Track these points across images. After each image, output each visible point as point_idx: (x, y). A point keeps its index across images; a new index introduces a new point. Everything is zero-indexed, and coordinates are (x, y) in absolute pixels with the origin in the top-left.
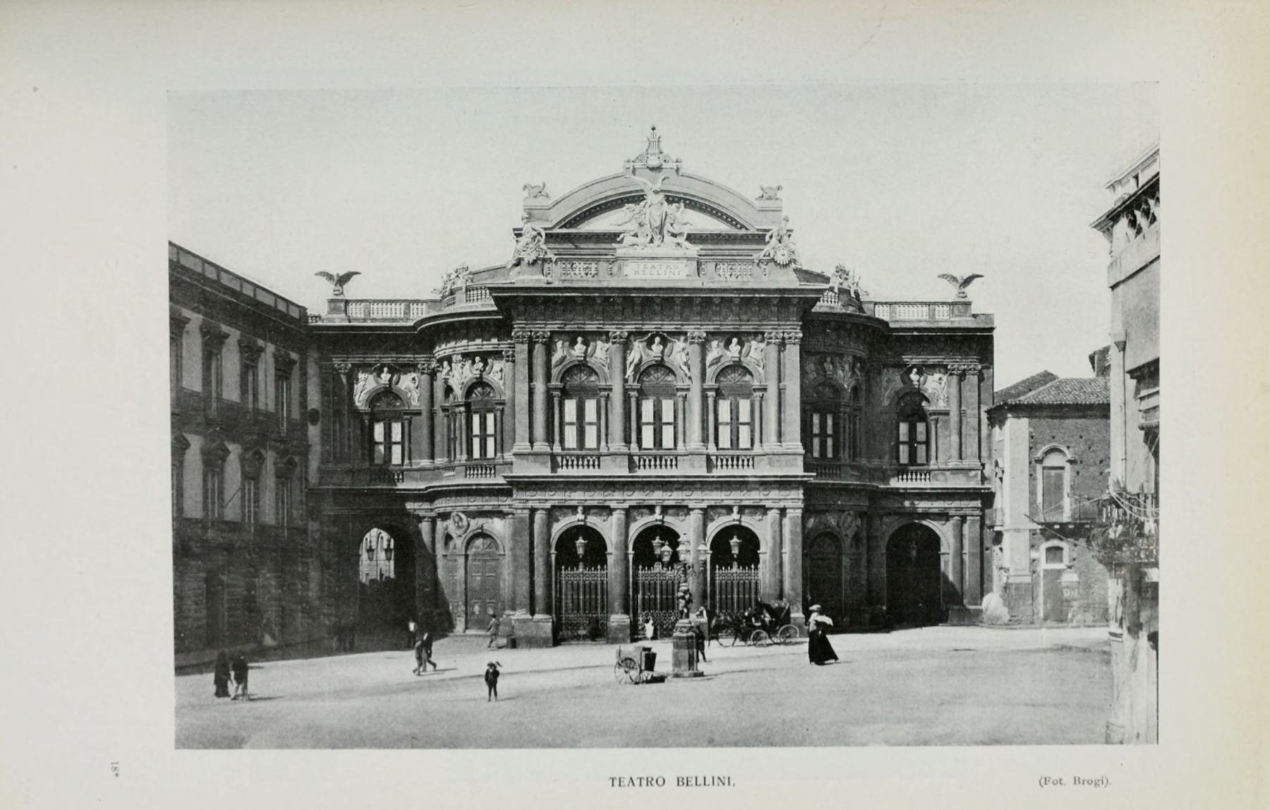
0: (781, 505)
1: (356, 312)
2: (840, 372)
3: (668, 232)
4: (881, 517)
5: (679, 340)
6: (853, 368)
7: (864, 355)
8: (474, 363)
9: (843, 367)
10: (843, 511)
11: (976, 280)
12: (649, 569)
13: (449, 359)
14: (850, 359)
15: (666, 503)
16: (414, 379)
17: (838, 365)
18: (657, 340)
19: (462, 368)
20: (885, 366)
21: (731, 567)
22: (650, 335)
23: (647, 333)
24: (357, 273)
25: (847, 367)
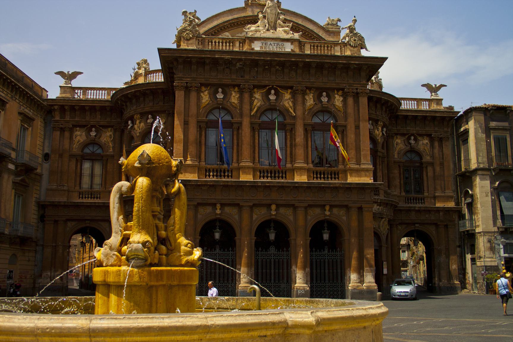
1: (79, 95)
2: (376, 131)
3: (280, 25)
5: (287, 93)
6: (382, 130)
7: (387, 123)
8: (148, 118)
9: (378, 128)
11: (443, 88)
12: (266, 251)
14: (382, 124)
16: (111, 135)
17: (375, 127)
18: (273, 92)
19: (140, 123)
23: (265, 87)
24: (81, 73)
25: (380, 128)
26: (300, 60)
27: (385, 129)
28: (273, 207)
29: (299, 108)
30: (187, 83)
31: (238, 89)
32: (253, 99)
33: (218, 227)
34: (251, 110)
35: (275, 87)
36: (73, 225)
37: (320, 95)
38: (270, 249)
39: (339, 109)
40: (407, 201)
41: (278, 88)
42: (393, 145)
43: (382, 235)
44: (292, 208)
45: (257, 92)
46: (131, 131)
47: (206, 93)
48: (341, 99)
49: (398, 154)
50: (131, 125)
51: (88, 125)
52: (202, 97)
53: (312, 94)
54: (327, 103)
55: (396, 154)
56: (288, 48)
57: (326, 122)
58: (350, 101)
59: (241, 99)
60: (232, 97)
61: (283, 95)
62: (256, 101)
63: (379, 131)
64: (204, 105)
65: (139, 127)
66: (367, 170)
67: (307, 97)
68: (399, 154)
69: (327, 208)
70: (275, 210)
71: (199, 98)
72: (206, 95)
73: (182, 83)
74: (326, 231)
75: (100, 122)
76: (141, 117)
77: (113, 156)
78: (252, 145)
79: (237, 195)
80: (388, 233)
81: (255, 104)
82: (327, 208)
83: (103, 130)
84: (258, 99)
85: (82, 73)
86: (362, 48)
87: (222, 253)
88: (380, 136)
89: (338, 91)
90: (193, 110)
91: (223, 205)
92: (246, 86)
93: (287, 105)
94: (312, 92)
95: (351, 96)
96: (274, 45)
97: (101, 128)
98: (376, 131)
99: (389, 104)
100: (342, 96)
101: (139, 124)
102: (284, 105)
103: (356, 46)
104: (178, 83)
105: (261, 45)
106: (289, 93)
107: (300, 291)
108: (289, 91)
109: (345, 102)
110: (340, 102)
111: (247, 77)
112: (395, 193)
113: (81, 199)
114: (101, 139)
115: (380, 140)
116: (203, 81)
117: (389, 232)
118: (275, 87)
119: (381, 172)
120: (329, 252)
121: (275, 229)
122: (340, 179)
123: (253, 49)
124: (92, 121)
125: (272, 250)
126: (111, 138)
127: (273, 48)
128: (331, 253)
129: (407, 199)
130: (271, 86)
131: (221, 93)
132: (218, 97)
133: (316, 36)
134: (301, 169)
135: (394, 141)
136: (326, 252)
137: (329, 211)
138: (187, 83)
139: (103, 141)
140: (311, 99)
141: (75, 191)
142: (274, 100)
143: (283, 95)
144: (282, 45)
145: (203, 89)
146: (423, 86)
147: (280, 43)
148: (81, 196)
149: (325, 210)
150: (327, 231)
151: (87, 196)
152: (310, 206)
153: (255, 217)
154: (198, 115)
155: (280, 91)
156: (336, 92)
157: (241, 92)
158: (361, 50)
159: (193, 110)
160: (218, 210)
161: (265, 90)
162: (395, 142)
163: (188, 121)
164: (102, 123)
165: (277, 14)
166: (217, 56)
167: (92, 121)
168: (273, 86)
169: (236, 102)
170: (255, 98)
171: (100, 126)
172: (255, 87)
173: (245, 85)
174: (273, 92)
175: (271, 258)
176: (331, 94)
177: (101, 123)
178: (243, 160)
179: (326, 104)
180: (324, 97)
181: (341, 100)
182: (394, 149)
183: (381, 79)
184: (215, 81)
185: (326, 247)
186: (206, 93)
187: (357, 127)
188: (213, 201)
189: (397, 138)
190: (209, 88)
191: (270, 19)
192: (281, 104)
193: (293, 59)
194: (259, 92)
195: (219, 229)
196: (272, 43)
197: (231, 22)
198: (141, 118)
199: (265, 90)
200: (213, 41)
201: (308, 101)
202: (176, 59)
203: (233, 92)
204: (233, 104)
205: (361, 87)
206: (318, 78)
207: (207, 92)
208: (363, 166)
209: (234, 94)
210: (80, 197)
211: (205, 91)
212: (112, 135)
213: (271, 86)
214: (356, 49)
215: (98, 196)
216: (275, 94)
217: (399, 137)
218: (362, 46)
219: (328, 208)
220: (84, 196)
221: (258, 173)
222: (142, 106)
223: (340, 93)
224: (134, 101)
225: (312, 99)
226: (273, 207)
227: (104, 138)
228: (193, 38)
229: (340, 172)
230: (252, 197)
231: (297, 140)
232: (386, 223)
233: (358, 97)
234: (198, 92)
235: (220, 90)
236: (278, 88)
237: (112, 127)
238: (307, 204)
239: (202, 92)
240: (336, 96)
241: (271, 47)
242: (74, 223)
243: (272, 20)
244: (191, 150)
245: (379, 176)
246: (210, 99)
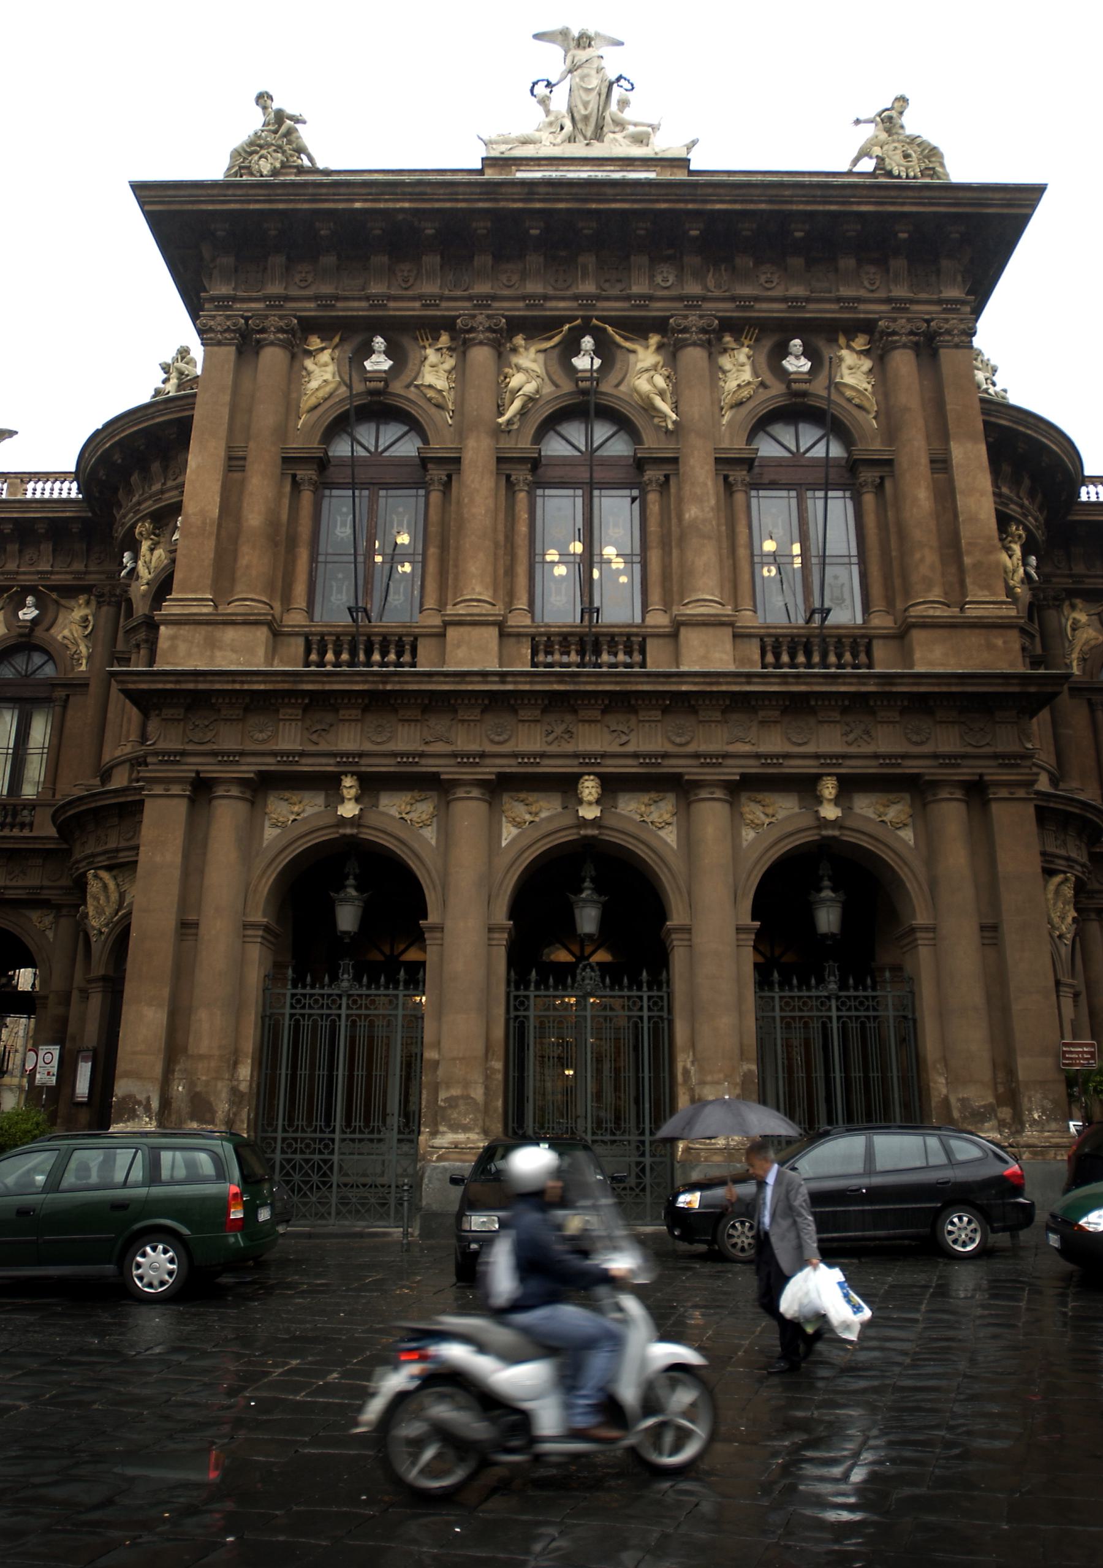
0: (966, 772)
2: (1004, 557)
5: (647, 347)
7: (1039, 535)
15: (611, 767)
16: (85, 619)
18: (588, 342)
20: (1072, 594)
21: (821, 981)
22: (567, 327)
25: (1017, 548)
27: (1033, 560)
28: (589, 788)
31: (452, 339)
33: (351, 881)
35: (595, 321)
37: (782, 351)
38: (579, 978)
39: (857, 401)
41: (609, 329)
42: (1062, 631)
45: (526, 349)
46: (129, 586)
48: (867, 364)
49: (1083, 660)
50: (130, 565)
51: (13, 586)
52: (309, 373)
53: (746, 350)
54: (807, 377)
55: (1075, 663)
58: (903, 362)
59: (460, 373)
61: (632, 357)
63: (1015, 558)
64: (313, 401)
65: (147, 565)
69: (829, 788)
70: (598, 802)
71: (295, 375)
72: (326, 365)
73: (228, 317)
74: (827, 894)
75: (52, 573)
76: (155, 528)
77: (87, 685)
78: (502, 542)
82: (829, 788)
83: (63, 602)
84: (526, 371)
85: (16, 433)
89: (850, 338)
90: (266, 417)
92: (480, 318)
94: (747, 342)
95: (905, 346)
97: (54, 596)
100: (866, 353)
101: (148, 553)
104: (213, 317)
106: (653, 348)
114: (52, 631)
116: (309, 309)
118: (595, 321)
120: (843, 986)
121: (598, 890)
124: (25, 573)
126: (86, 627)
130: (579, 321)
131: (383, 357)
135: (1063, 620)
137: (837, 801)
138: (247, 319)
139: (59, 638)
140: (743, 365)
145: (315, 342)
150: (832, 895)
153: (508, 833)
154: (282, 431)
155: (618, 338)
156: (842, 340)
157: (461, 345)
159: (266, 417)
161: (557, 339)
162: (1070, 623)
163: (244, 458)
164: (56, 579)
167: (25, 573)
168: (587, 319)
170: (519, 369)
171: (52, 588)
173: (473, 317)
174: (588, 342)
177: (53, 577)
180: (797, 357)
182: (1067, 644)
183: (1005, 391)
185: (831, 965)
186: (325, 357)
187: (941, 464)
188: (328, 766)
189: (1073, 607)
190: (337, 339)
191: (581, 107)
192: (623, 388)
194: (533, 350)
195: (357, 889)
199: (557, 339)
203: (430, 352)
204: (431, 394)
205: (946, 311)
206: (767, 285)
207: (327, 352)
208: (972, 611)
209: (432, 355)
211: (323, 349)
212: (90, 618)
213: (579, 321)
216: (597, 352)
217: (1078, 602)
219: (834, 792)
221: (524, 651)
222: (157, 487)
223: (860, 343)
225: (748, 369)
226: (589, 788)
227: (64, 629)
230: (492, 742)
231: (687, 516)
233: (934, 354)
234: (293, 357)
235: (379, 342)
236: (609, 329)
237: (87, 590)
239: (309, 354)
243: (586, 113)
246: (341, 377)
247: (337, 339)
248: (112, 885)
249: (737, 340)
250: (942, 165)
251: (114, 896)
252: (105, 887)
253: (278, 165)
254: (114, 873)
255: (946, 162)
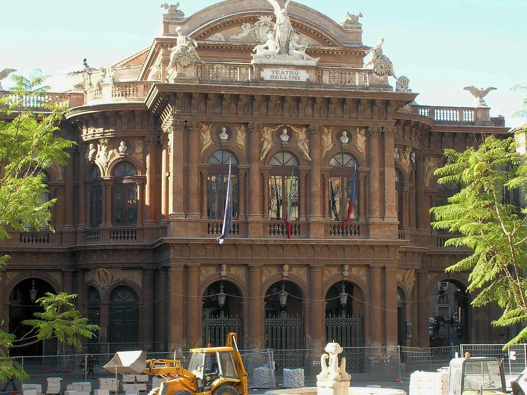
2: (403, 160)
4: (426, 273)
9: (405, 156)
10: (407, 269)
11: (491, 92)
13: (96, 142)
18: (285, 131)
25: (408, 156)
26: (318, 96)
27: (414, 155)
29: (317, 153)
30: (186, 122)
32: (262, 140)
34: (261, 153)
35: (288, 125)
36: (13, 277)
37: (339, 136)
38: (281, 315)
40: (439, 243)
41: (292, 127)
43: (407, 290)
44: (306, 269)
45: (267, 131)
47: (208, 132)
48: (364, 139)
55: (427, 182)
56: (303, 76)
57: (345, 166)
58: (375, 143)
59: (248, 140)
60: (238, 138)
62: (266, 143)
63: (407, 159)
66: (392, 224)
67: (323, 137)
68: (431, 181)
74: (344, 293)
79: (245, 255)
80: (415, 286)
81: (265, 147)
85: (16, 70)
86: (389, 75)
87: (227, 319)
88: (407, 165)
90: (194, 155)
91: (229, 266)
93: (302, 147)
94: (330, 131)
96: (287, 74)
98: (403, 160)
99: (421, 125)
102: (297, 147)
103: (382, 74)
105: (271, 74)
107: (315, 362)
108: (304, 130)
109: (368, 142)
110: (363, 143)
111: (256, 114)
112: (425, 233)
113: (23, 242)
115: (407, 171)
117: (416, 285)
118: (288, 125)
119: (408, 211)
120: (347, 317)
122: (360, 234)
123: (262, 79)
125: (284, 315)
127: (285, 75)
128: (348, 319)
129: (439, 240)
132: (222, 138)
133: (332, 40)
134: (317, 223)
135: (425, 165)
136: (344, 316)
141: (15, 233)
142: (286, 141)
143: (297, 134)
144: (296, 73)
145: (205, 127)
146: (466, 88)
147: (294, 71)
148: (23, 239)
149: (344, 270)
150: (345, 294)
151: (31, 239)
152: (327, 266)
153: (264, 278)
155: (294, 129)
158: (388, 76)
160: (224, 272)
161: (276, 129)
165: (290, 32)
166: (222, 92)
168: (285, 124)
169: (243, 144)
172: (265, 125)
175: (282, 325)
176: (352, 132)
178: (251, 213)
179: (347, 146)
181: (364, 140)
184: (219, 119)
187: (382, 174)
190: (211, 126)
191: (282, 38)
193: (311, 96)
194: (269, 131)
196: (284, 71)
197: (225, 20)
198: (110, 143)
200: (215, 67)
201: (326, 142)
202: (175, 94)
204: (240, 146)
208: (387, 220)
210: (21, 241)
214: (382, 78)
215: (46, 238)
217: (432, 159)
218: (390, 73)
220: (27, 239)
221: (267, 228)
223: (363, 131)
224: (100, 121)
225: (330, 140)
226: (286, 267)
228: (191, 65)
229: (361, 226)
231: (312, 190)
232: (412, 275)
236: (292, 127)
238: (324, 264)
240: (358, 135)
241: (283, 75)
242: (15, 274)
244: (192, 203)
245: (405, 217)
247: (211, 126)
248: (109, 274)
249: (328, 129)
250: (392, 69)
251: (110, 278)
252: (106, 273)
253: (189, 63)
254: (109, 269)
255: (394, 67)
